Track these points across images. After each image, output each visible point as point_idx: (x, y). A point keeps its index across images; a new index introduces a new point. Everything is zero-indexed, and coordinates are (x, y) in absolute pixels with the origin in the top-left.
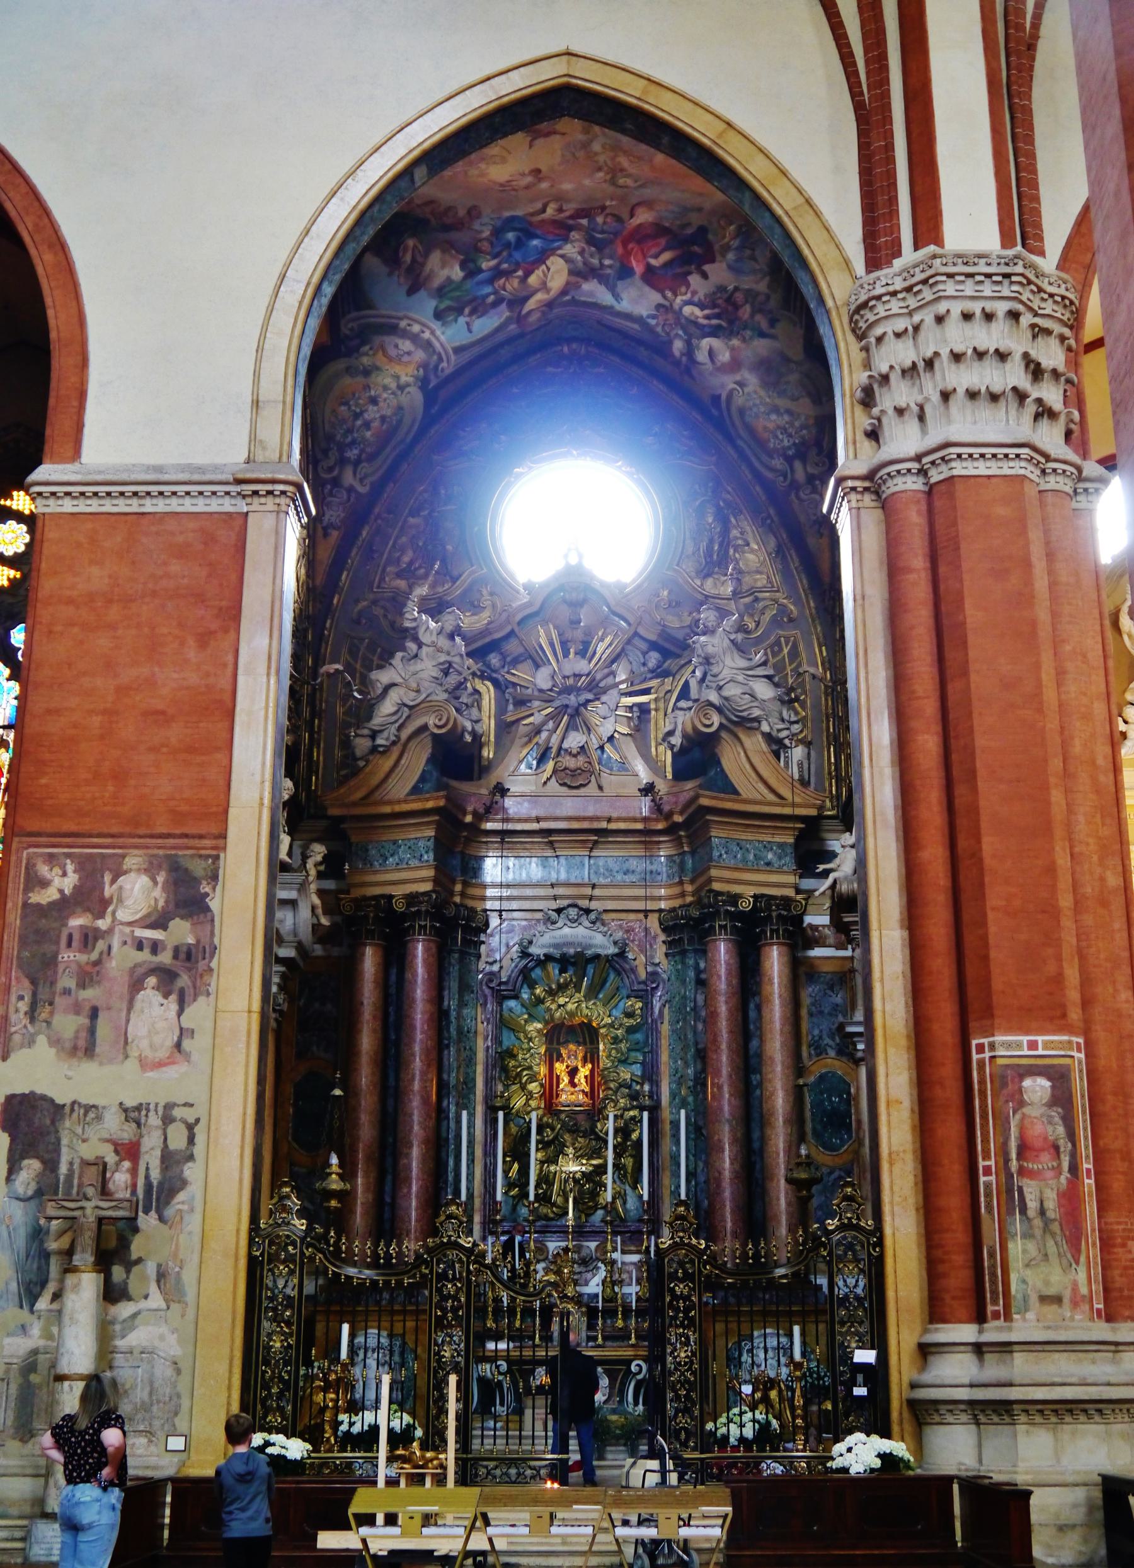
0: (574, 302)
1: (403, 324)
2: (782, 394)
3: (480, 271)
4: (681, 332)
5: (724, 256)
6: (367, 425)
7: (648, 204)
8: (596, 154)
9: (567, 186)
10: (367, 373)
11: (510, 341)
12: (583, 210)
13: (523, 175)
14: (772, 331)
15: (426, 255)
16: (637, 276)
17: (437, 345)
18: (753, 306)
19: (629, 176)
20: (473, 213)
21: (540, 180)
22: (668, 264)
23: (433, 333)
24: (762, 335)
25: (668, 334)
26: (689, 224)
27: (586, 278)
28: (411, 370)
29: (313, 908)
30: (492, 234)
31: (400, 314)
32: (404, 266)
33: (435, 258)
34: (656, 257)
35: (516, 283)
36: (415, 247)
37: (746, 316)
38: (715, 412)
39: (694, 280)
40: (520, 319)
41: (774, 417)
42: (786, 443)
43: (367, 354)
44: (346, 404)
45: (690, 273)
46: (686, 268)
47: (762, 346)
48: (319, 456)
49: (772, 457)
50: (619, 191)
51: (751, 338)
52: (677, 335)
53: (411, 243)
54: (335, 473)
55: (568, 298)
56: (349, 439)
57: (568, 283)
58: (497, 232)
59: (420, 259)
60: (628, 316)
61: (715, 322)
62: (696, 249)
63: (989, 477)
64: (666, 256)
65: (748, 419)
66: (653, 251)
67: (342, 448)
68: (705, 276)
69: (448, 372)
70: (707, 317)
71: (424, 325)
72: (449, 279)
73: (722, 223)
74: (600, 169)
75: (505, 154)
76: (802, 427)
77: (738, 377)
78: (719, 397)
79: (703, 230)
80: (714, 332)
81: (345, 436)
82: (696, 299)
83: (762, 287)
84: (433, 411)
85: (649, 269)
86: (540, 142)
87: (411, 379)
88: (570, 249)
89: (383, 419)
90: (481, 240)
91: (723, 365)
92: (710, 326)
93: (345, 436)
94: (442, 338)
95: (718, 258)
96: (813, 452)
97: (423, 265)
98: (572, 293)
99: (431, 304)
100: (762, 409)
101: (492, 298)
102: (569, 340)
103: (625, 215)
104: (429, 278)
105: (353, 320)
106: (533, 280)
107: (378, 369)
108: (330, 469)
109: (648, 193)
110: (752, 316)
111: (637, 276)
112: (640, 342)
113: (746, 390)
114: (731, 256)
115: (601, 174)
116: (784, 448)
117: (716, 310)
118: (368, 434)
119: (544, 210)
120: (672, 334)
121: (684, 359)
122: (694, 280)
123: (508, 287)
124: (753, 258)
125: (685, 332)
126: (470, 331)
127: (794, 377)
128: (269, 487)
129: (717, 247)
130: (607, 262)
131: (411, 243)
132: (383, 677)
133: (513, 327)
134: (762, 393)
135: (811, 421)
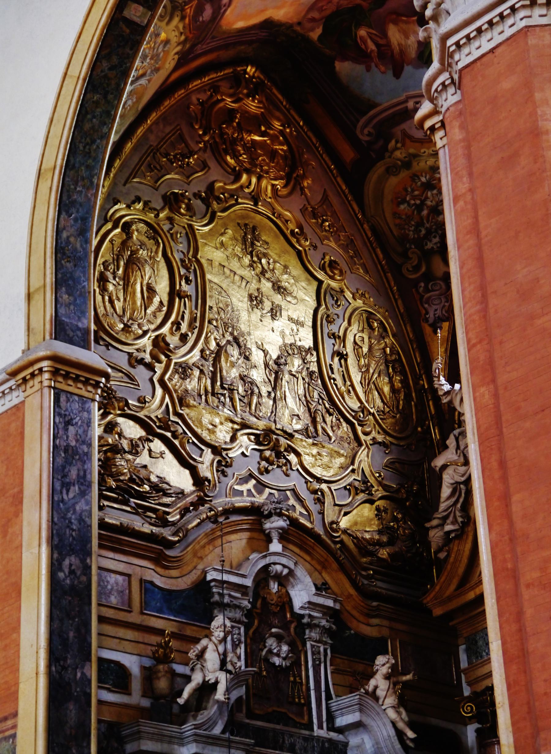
10: (407, 164)
15: (385, 35)
29: (394, 724)
31: (403, 97)
36: (368, 33)
43: (396, 149)
44: (404, 201)
53: (362, 32)
54: (424, 269)
56: (423, 232)
59: (382, 42)
63: (492, 50)
81: (417, 230)
97: (389, 44)
107: (415, 156)
108: (417, 268)
128: (30, 370)
132: (439, 462)
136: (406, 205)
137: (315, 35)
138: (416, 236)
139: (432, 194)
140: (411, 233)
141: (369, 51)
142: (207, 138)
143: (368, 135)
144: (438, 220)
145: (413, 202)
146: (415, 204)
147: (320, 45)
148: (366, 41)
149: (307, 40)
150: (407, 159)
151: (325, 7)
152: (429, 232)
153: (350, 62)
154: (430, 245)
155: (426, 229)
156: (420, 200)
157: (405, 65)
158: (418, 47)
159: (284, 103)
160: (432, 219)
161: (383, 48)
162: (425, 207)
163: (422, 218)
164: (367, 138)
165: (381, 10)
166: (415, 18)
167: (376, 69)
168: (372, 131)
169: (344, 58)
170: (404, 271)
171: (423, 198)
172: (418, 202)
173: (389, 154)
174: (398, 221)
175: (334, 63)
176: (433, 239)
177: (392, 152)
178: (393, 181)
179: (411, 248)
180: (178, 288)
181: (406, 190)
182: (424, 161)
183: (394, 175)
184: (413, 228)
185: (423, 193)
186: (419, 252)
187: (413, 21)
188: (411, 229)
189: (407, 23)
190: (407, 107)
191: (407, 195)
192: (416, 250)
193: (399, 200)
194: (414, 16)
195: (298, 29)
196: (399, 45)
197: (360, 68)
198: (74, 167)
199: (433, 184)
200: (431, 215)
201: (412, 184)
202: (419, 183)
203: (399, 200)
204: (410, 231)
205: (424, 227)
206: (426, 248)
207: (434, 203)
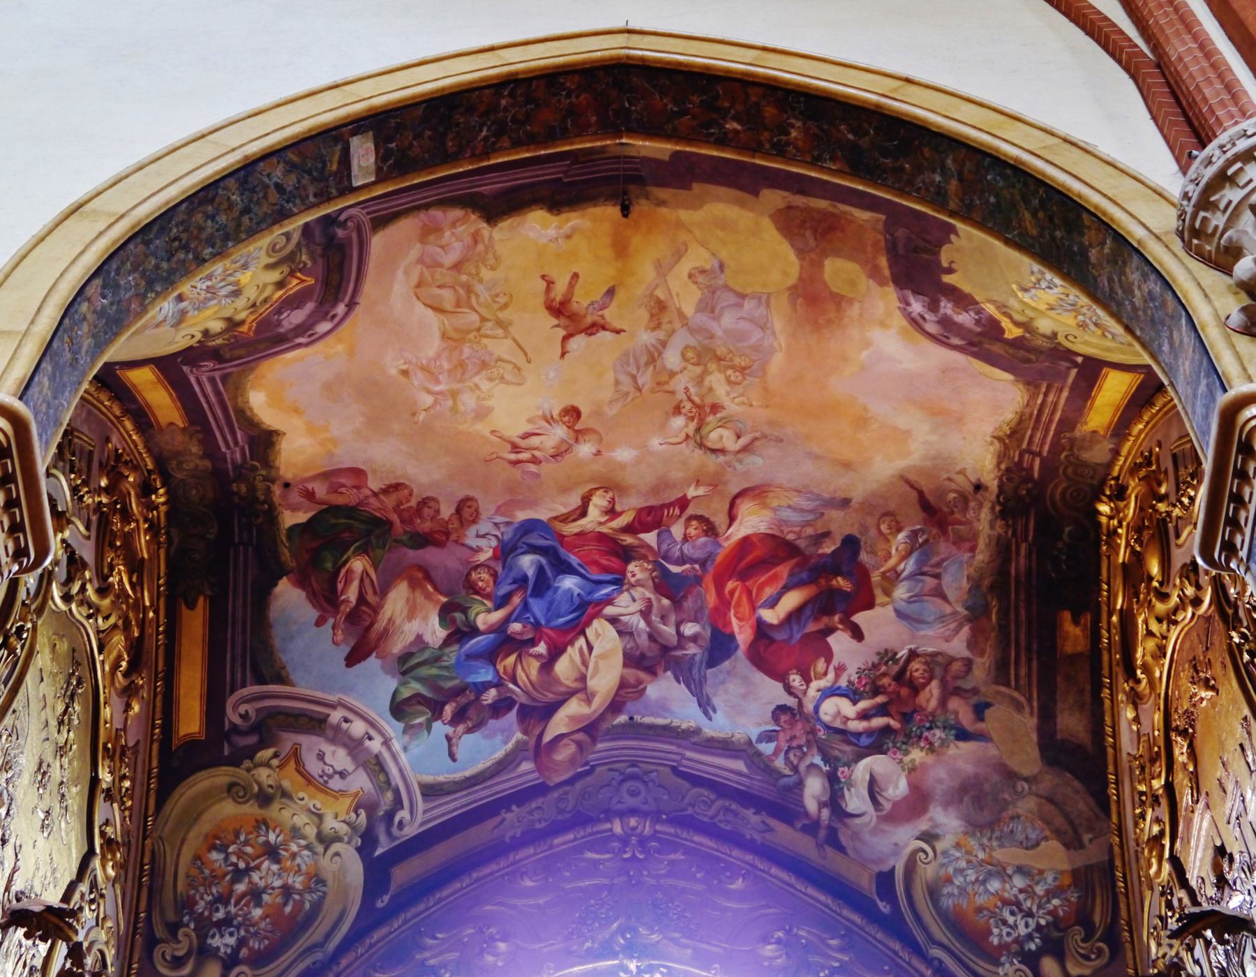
0: (634, 730)
1: (336, 716)
2: (1007, 839)
3: (474, 631)
4: (818, 760)
5: (888, 593)
6: (255, 895)
7: (756, 492)
8: (672, 374)
9: (623, 454)
10: (265, 799)
11: (522, 797)
12: (650, 510)
13: (549, 420)
14: (981, 726)
15: (383, 592)
16: (740, 653)
17: (394, 771)
18: (943, 684)
19: (724, 424)
20: (466, 511)
21: (579, 435)
22: (794, 616)
23: (387, 743)
24: (963, 735)
25: (795, 769)
26: (827, 534)
27: (652, 672)
28: (345, 804)
30: (495, 557)
31: (333, 698)
32: (346, 609)
33: (397, 600)
34: (773, 603)
35: (534, 666)
36: (365, 572)
37: (933, 703)
38: (884, 907)
39: (840, 642)
40: (540, 751)
41: (994, 885)
42: (1022, 931)
43: (267, 765)
44: (223, 849)
45: (831, 630)
46: (825, 620)
47: (963, 756)
48: (160, 932)
49: (998, 963)
50: (713, 462)
51: (944, 743)
52: (812, 765)
53: (358, 565)
55: (623, 718)
56: (220, 915)
57: (623, 684)
58: (505, 552)
59: (371, 598)
60: (724, 747)
61: (878, 722)
62: (841, 582)
64: (792, 600)
65: (947, 903)
66: (769, 592)
67: (205, 927)
68: (857, 634)
69: (410, 831)
70: (863, 716)
71: (372, 724)
72: (419, 638)
73: (884, 528)
74: (677, 410)
75: (521, 361)
76: (1050, 894)
77: (923, 825)
78: (893, 870)
79: (851, 544)
80: (878, 743)
81: (213, 906)
82: (843, 683)
83: (958, 646)
84: (380, 905)
85: (762, 631)
86: (578, 343)
87: (343, 829)
88: (626, 605)
89: (287, 891)
90: (476, 567)
91: (896, 805)
92: (869, 732)
93: (213, 906)
94: (403, 758)
95: (880, 598)
96: (1077, 933)
97: (376, 610)
98: (630, 706)
99: (387, 685)
100: (972, 876)
101: (491, 695)
102: (623, 814)
103: (720, 520)
104: (385, 634)
105: (248, 701)
106: (564, 667)
107: (285, 794)
109: (757, 466)
110: (943, 703)
111: (740, 653)
112: (746, 798)
113: (940, 846)
114: (901, 592)
115: (679, 422)
116: (1017, 941)
117: (880, 699)
118: (257, 913)
119: (582, 512)
120: (802, 768)
121: (826, 813)
122: (840, 642)
123: (520, 674)
124: (939, 593)
125: (826, 759)
126: (452, 757)
127: (1026, 805)
129: (875, 577)
130: (690, 629)
131: (358, 565)
133: (527, 766)
134: (972, 843)
135: (1067, 880)
136: (221, 856)
137: (289, 519)
138: (206, 913)
139: (269, 869)
140: (202, 903)
141: (343, 597)
142: (105, 500)
143: (241, 716)
144: (250, 913)
145: (234, 859)
146: (236, 865)
147: (284, 539)
148: (351, 581)
149: (272, 517)
150: (270, 790)
151: (343, 490)
152: (227, 922)
153: (303, 594)
154: (215, 942)
155: (228, 913)
156: (247, 864)
157: (374, 654)
158: (411, 644)
159: (161, 582)
160: (244, 905)
161: (364, 608)
162: (247, 880)
163: (231, 892)
164: (237, 720)
165: (411, 553)
166: (444, 600)
167: (331, 631)
168: (252, 713)
169: (301, 583)
170: (157, 953)
171: (252, 864)
172: (242, 865)
173: (251, 765)
174: (194, 872)
175: (280, 578)
176: (227, 935)
177: (257, 766)
178: (228, 809)
179: (187, 926)
180: (8, 627)
181: (237, 835)
182: (293, 812)
183: (234, 800)
184: (210, 898)
185: (258, 857)
186: (195, 941)
187: (438, 601)
188: (205, 897)
189: (428, 596)
190: (328, 715)
191: (234, 843)
192: (193, 934)
193: (218, 842)
194: (445, 595)
195: (277, 490)
196: (390, 620)
197: (312, 614)
198: (147, 243)
199: (279, 854)
200: (249, 897)
201: (251, 833)
202: (262, 839)
203: (218, 842)
204: (202, 898)
205: (226, 907)
206: (209, 941)
207: (262, 884)
